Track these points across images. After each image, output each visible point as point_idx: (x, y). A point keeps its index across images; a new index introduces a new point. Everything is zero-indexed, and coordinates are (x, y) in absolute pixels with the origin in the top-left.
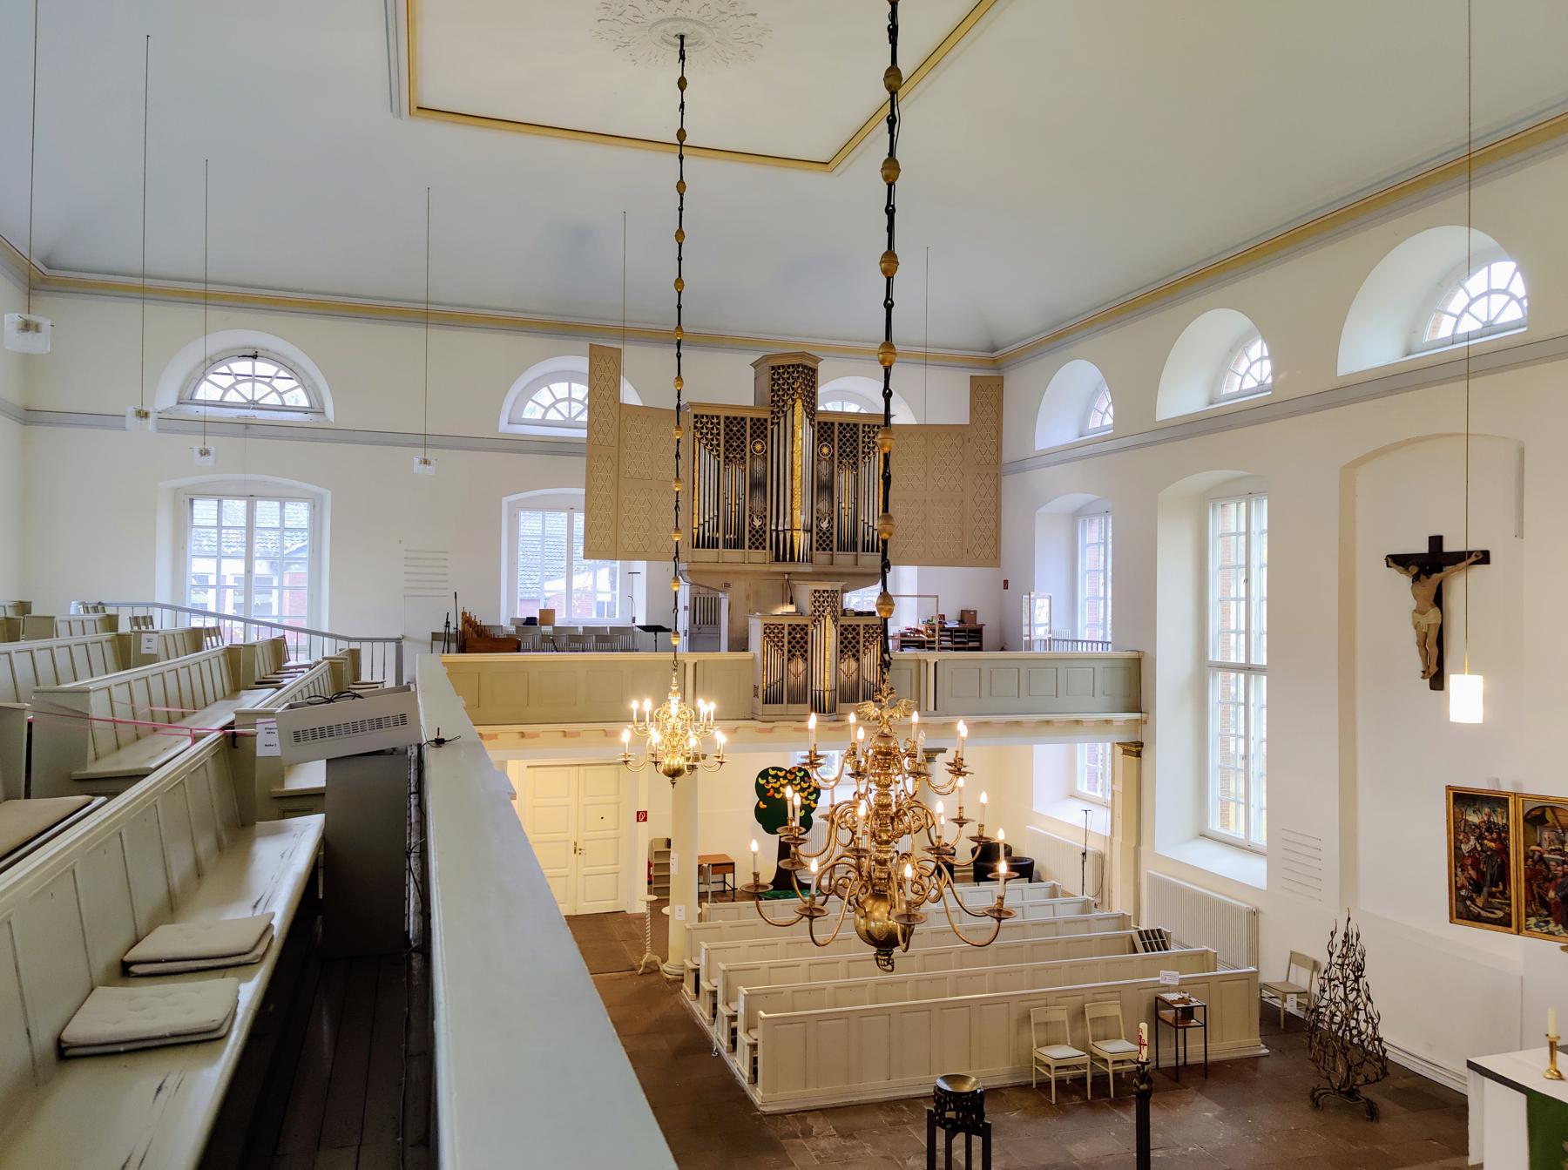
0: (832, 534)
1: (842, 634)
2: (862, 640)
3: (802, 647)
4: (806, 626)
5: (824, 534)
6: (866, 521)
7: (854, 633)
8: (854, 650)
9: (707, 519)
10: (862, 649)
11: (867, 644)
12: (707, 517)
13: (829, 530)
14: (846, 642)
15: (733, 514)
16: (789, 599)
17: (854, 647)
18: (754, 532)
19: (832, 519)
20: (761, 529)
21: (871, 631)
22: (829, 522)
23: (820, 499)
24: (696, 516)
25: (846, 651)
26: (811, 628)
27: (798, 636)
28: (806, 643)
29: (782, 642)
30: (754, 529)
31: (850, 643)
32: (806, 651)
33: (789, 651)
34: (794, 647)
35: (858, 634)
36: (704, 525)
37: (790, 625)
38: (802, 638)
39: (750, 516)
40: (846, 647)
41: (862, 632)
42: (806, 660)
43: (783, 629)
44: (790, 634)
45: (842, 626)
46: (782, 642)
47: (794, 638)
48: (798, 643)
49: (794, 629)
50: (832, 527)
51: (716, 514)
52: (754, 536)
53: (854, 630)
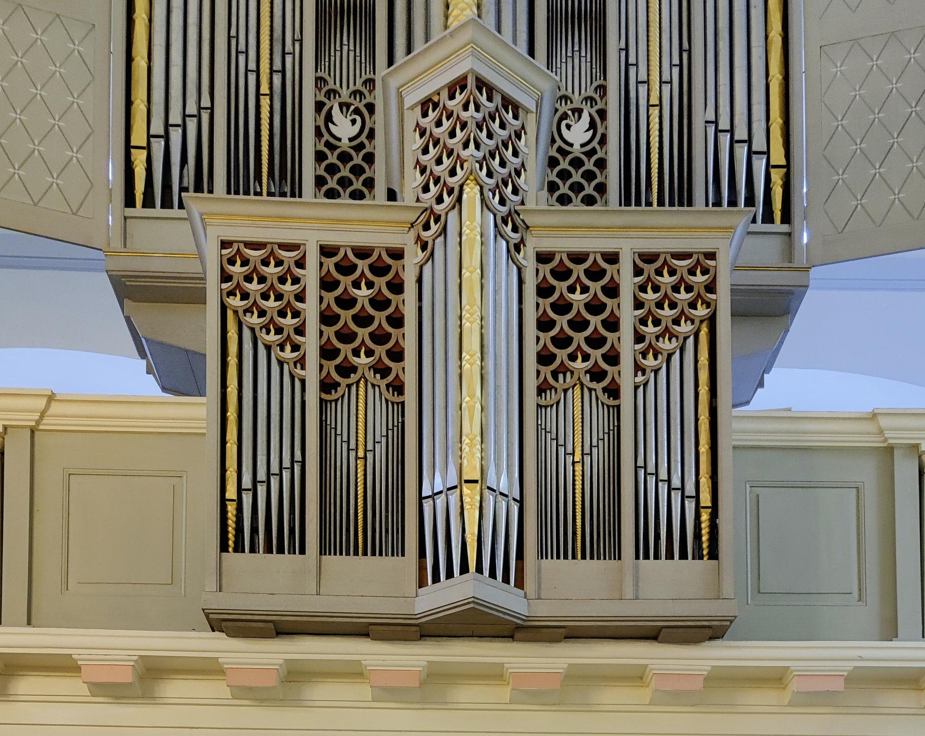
0: (601, 164)
1: (544, 291)
2: (628, 316)
3: (380, 338)
4: (397, 254)
5: (577, 163)
6: (724, 124)
7: (595, 287)
8: (596, 354)
9: (176, 118)
10: (627, 349)
11: (650, 329)
12: (176, 118)
13: (593, 152)
14: (562, 321)
15: (265, 102)
16: (336, 194)
17: (596, 341)
18: (332, 158)
19: (602, 114)
20: (361, 147)
21: (667, 280)
22: (592, 125)
23: (561, 53)
24: (139, 107)
25: (562, 355)
26: (413, 256)
27: (364, 293)
28: (397, 321)
29: (296, 314)
30: (331, 147)
31: (579, 325)
32: (397, 355)
33: (327, 353)
34: (346, 337)
35: (612, 291)
36: (167, 137)
37: (327, 251)
38: (379, 303)
39: (319, 106)
40: (562, 341)
41: (627, 283)
42: (398, 387)
43: (301, 264)
44: (327, 284)
45: (543, 258)
46: (296, 314)
47: (347, 302)
48: (363, 320)
49: (346, 269)
50: (603, 141)
51: (206, 102)
52: (332, 169)
53: (595, 274)
